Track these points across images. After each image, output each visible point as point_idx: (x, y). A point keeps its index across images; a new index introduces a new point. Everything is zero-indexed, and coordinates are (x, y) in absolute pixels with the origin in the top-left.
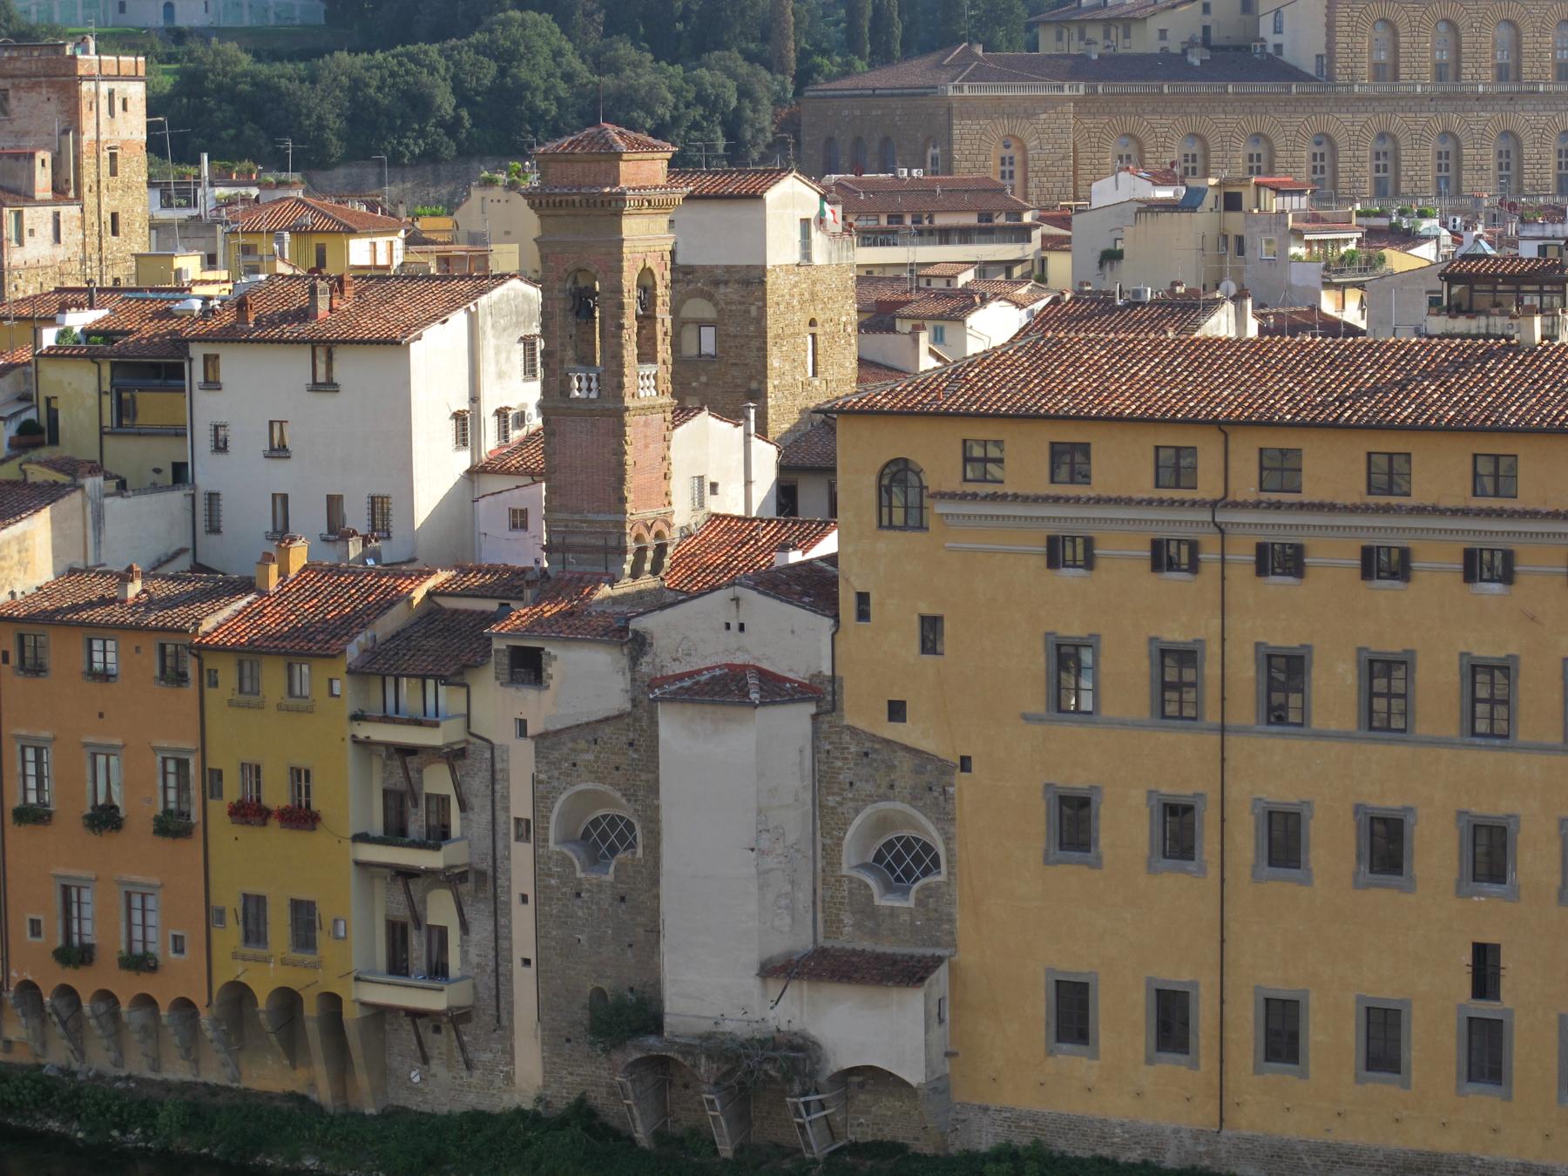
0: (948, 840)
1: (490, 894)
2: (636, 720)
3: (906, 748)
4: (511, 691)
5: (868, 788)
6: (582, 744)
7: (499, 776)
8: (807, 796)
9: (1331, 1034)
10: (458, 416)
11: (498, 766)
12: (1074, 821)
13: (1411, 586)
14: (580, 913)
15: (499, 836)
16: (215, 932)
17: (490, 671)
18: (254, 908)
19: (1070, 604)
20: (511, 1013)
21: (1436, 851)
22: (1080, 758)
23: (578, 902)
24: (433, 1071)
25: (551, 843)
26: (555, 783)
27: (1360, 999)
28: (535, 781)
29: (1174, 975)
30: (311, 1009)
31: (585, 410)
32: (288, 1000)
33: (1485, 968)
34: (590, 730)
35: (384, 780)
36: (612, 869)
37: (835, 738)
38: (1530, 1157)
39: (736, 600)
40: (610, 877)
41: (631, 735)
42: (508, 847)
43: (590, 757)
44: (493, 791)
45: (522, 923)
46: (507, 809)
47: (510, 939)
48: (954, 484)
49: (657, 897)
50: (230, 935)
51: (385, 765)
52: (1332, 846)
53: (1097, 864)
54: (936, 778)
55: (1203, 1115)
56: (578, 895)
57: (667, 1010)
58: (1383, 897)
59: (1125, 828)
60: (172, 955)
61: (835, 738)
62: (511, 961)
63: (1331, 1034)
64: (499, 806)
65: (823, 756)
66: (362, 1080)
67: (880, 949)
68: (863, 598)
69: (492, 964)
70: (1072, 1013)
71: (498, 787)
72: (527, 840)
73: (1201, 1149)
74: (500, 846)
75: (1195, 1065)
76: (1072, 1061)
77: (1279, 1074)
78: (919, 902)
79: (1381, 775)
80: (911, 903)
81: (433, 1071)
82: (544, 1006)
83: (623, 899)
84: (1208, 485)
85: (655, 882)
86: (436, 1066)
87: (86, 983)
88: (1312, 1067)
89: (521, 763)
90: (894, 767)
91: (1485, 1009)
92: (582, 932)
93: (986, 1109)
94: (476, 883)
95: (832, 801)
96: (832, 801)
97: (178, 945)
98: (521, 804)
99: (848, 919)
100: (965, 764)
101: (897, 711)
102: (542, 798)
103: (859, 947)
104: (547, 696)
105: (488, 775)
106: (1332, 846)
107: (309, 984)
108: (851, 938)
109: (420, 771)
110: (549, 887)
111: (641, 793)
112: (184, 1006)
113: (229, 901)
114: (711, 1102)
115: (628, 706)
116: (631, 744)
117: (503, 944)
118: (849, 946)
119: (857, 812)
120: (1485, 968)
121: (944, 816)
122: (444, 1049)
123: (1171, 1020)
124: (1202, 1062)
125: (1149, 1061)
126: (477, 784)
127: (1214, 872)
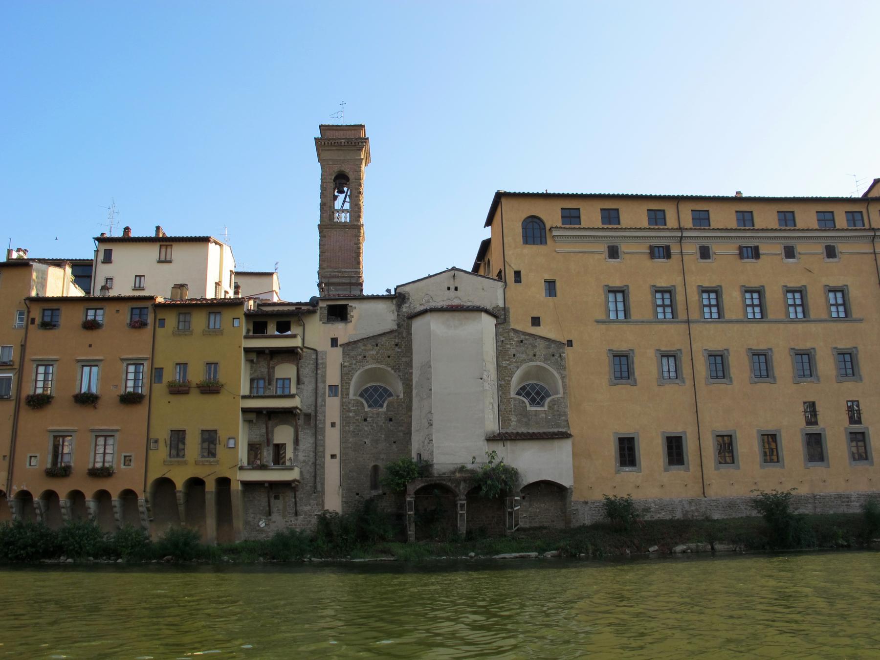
0: (563, 378)
1: (312, 425)
2: (399, 333)
3: (541, 337)
4: (329, 325)
5: (524, 356)
6: (369, 347)
7: (320, 366)
8: (495, 360)
9: (748, 447)
10: (216, 283)
11: (320, 361)
12: (622, 365)
13: (759, 261)
14: (366, 429)
15: (320, 394)
16: (151, 453)
17: (317, 316)
18: (178, 438)
19: (615, 273)
20: (323, 484)
21: (783, 365)
22: (625, 338)
23: (366, 423)
24: (274, 520)
25: (351, 396)
26: (354, 366)
27: (758, 431)
28: (342, 366)
29: (675, 429)
30: (210, 487)
31: (344, 226)
32: (196, 484)
33: (811, 410)
34: (374, 340)
35: (251, 374)
36: (385, 405)
37: (506, 335)
38: (841, 491)
39: (454, 276)
40: (384, 409)
41: (397, 341)
42: (324, 400)
43: (374, 352)
44: (317, 374)
45: (332, 440)
46: (324, 382)
47: (324, 446)
48: (559, 224)
49: (411, 417)
50: (162, 453)
51: (252, 367)
52: (739, 366)
53: (635, 383)
54: (557, 349)
55: (693, 492)
56: (365, 420)
57: (435, 461)
58: (763, 387)
59: (646, 366)
60: (122, 466)
61: (506, 335)
62: (324, 457)
63: (748, 447)
64: (319, 380)
65: (500, 343)
66: (238, 523)
67: (531, 431)
68: (518, 274)
69: (312, 460)
70: (627, 452)
71: (319, 372)
72: (336, 395)
73: (693, 508)
74: (319, 400)
75: (687, 470)
76: (629, 475)
77: (725, 470)
78: (549, 407)
79: (758, 336)
80: (546, 408)
81: (274, 520)
82: (345, 478)
83: (391, 420)
84: (671, 222)
85: (410, 409)
86: (275, 517)
87: (63, 488)
88: (741, 464)
89: (334, 359)
90: (536, 346)
91: (813, 429)
92: (367, 438)
93: (586, 503)
94: (304, 420)
95: (504, 363)
96: (504, 363)
97: (127, 460)
98: (333, 377)
99: (513, 418)
100: (570, 343)
101: (536, 321)
102: (346, 374)
103: (520, 431)
104: (350, 326)
105: (312, 367)
106: (739, 366)
107: (209, 475)
108: (515, 426)
109: (274, 368)
110: (349, 417)
111: (401, 368)
112: (128, 495)
113: (162, 433)
114: (462, 506)
115: (395, 327)
116: (396, 345)
117: (320, 449)
118: (514, 431)
119: (518, 368)
120: (811, 410)
121: (561, 366)
122: (281, 507)
123: (675, 449)
124: (691, 467)
125: (666, 470)
126: (307, 371)
127: (689, 383)
